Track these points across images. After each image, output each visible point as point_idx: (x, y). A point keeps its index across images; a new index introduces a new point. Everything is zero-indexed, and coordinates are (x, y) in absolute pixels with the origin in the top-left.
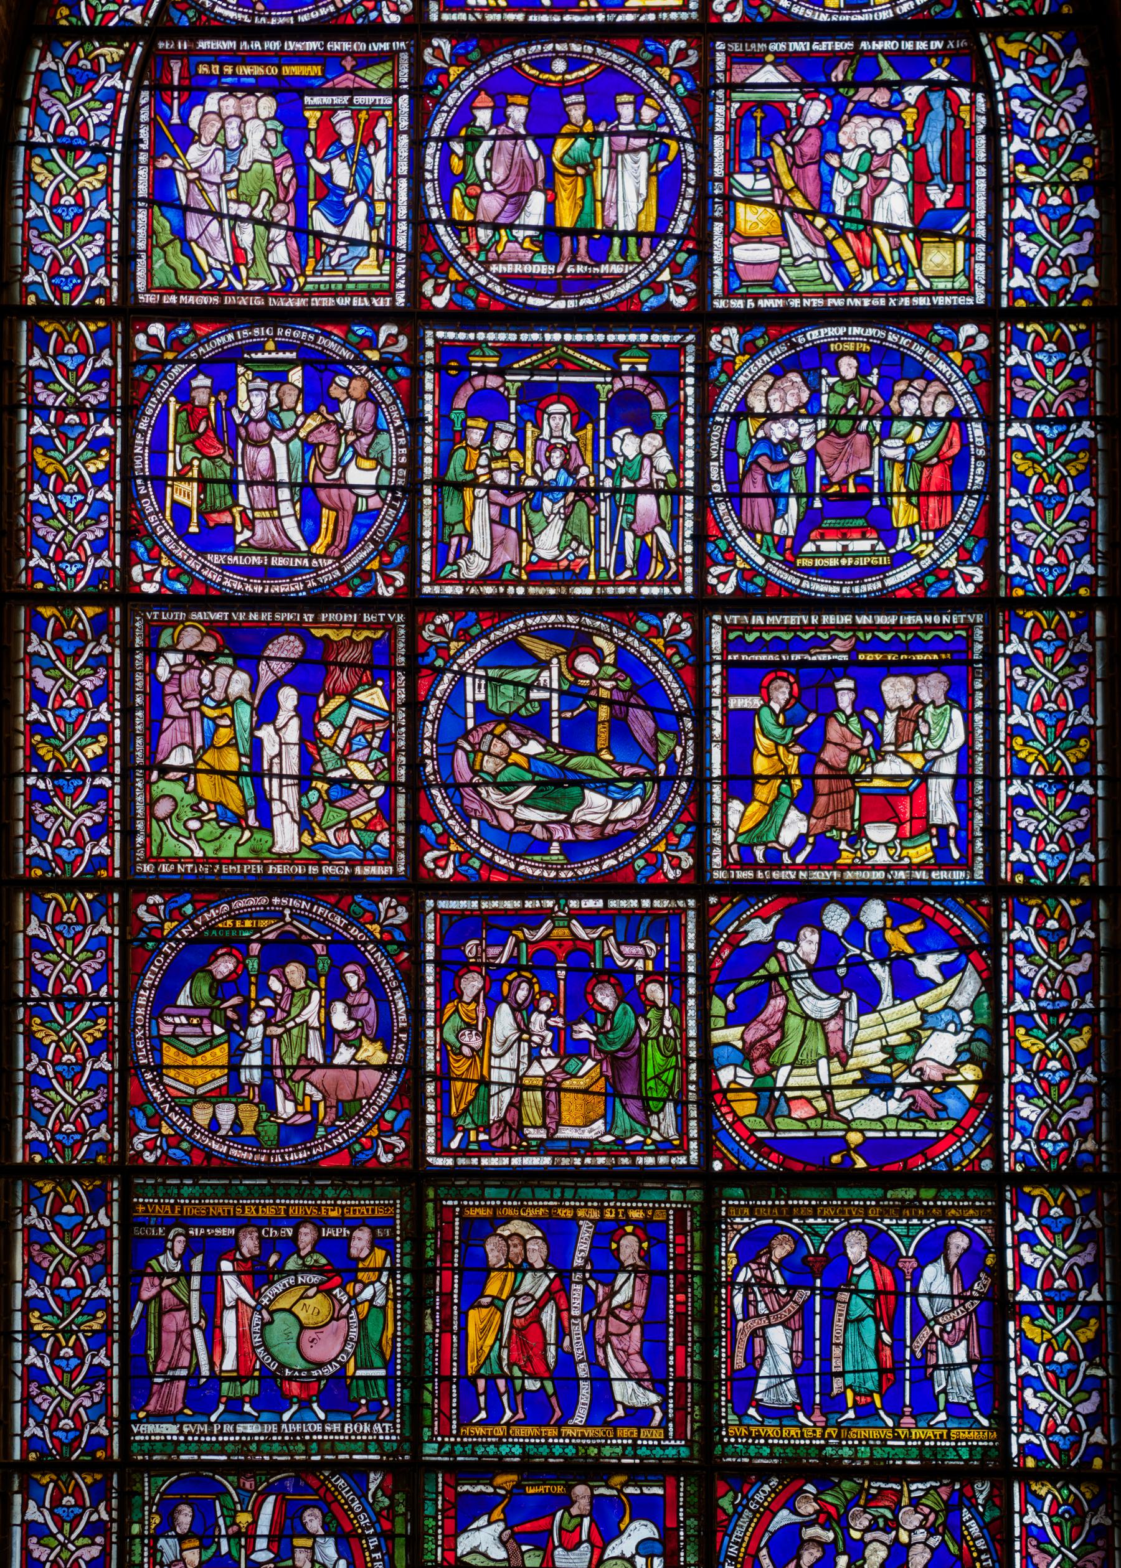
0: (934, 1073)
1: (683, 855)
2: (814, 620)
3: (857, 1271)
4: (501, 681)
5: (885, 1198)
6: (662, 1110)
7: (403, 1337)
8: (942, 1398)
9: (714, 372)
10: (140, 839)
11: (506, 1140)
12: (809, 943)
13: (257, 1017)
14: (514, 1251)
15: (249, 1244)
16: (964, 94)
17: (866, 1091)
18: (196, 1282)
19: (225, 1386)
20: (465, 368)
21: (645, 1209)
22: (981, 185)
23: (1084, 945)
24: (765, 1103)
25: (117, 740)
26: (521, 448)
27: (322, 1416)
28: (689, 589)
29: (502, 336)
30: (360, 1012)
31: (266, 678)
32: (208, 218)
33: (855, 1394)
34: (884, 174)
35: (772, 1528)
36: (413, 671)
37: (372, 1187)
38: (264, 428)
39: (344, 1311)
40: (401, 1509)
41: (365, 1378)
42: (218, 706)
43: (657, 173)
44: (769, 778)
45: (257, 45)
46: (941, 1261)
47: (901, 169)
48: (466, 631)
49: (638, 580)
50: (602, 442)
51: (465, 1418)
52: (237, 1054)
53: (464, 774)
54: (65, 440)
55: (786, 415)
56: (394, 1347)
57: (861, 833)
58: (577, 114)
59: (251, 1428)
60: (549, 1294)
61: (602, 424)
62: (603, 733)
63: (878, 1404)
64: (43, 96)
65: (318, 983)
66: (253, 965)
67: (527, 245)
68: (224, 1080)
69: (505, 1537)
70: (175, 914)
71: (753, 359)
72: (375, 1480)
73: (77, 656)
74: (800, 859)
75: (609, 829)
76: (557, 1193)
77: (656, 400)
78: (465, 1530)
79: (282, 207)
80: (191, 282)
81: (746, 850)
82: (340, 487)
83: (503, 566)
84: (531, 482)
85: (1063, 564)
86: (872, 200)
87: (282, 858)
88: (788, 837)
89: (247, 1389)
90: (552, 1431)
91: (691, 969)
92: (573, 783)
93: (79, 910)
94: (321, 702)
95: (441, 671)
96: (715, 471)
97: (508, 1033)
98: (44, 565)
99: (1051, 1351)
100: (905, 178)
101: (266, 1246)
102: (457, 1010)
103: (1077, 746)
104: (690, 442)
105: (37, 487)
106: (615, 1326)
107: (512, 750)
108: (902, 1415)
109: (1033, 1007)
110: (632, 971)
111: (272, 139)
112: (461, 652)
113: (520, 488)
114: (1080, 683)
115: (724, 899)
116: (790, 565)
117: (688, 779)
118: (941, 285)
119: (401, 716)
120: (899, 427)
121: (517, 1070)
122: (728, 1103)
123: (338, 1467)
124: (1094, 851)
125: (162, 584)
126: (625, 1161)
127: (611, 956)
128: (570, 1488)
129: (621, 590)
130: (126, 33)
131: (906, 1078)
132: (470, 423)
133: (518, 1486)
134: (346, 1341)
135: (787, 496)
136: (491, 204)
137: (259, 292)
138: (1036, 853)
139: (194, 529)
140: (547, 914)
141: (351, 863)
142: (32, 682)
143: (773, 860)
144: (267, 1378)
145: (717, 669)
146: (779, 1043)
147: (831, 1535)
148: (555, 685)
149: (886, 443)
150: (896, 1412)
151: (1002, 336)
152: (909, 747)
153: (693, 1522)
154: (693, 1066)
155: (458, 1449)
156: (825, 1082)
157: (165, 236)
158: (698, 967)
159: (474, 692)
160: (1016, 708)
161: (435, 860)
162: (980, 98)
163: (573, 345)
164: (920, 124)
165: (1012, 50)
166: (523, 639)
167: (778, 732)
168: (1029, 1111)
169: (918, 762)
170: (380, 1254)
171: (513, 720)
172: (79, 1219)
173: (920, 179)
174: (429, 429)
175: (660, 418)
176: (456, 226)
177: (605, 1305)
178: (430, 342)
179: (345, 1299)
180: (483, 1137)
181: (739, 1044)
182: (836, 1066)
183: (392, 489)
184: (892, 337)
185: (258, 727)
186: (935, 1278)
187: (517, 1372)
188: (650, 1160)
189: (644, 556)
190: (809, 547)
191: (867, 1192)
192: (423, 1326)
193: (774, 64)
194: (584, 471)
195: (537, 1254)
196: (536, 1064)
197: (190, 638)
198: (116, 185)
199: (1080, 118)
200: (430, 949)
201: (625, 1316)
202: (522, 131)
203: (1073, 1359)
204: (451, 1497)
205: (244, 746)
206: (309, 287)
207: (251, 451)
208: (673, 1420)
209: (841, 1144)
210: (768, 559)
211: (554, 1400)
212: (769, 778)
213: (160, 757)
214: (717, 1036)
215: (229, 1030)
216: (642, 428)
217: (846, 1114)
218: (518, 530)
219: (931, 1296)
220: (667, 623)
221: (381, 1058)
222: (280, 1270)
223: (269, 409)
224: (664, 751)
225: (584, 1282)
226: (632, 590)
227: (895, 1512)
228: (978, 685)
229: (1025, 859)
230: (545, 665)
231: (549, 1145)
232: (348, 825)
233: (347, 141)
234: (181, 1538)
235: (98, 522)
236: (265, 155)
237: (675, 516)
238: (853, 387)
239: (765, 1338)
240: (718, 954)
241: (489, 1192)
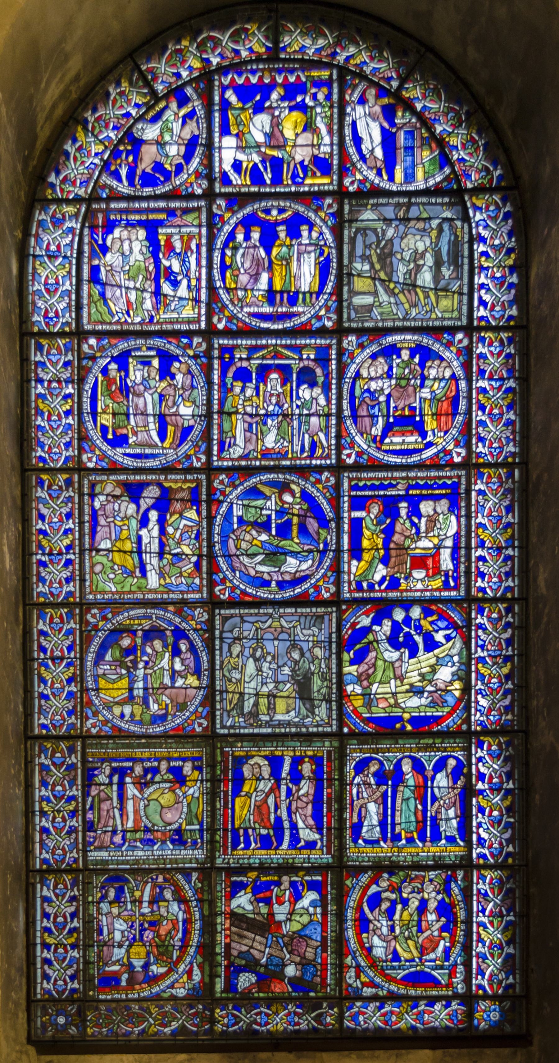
0: (442, 686)
1: (331, 586)
2: (390, 475)
3: (407, 777)
4: (248, 506)
7: (207, 811)
9: (345, 358)
10: (88, 583)
12: (387, 626)
13: (141, 665)
14: (256, 771)
15: (138, 770)
16: (459, 223)
17: (411, 694)
18: (115, 787)
20: (232, 358)
22: (466, 268)
23: (508, 625)
24: (367, 700)
25: (77, 536)
26: (258, 394)
27: (171, 847)
28: (334, 461)
29: (249, 342)
30: (187, 662)
31: (143, 507)
32: (115, 288)
33: (406, 832)
34: (421, 262)
36: (209, 502)
37: (192, 742)
38: (142, 388)
41: (190, 831)
42: (122, 520)
43: (320, 263)
44: (369, 550)
45: (137, 205)
47: (429, 260)
48: (233, 483)
49: (311, 457)
50: (294, 392)
51: (234, 847)
52: (132, 682)
53: (233, 550)
54: (51, 394)
55: (377, 378)
57: (410, 575)
58: (282, 235)
59: (140, 853)
60: (271, 790)
61: (294, 384)
62: (295, 529)
63: (416, 836)
64: (40, 231)
65: (167, 648)
66: (139, 641)
67: (260, 298)
68: (127, 695)
70: (104, 618)
71: (362, 352)
72: (195, 876)
73: (58, 498)
74: (383, 587)
75: (297, 575)
76: (275, 744)
77: (319, 371)
79: (149, 282)
80: (107, 318)
81: (359, 584)
82: (176, 415)
83: (250, 452)
84: (262, 412)
85: (501, 447)
86: (416, 275)
87: (151, 591)
88: (377, 577)
89: (138, 835)
90: (272, 852)
92: (282, 554)
93: (61, 617)
94: (168, 517)
95: (222, 502)
96: (345, 404)
98: (43, 455)
99: (491, 811)
100: (431, 265)
101: (146, 771)
103: (506, 532)
104: (334, 391)
105: (39, 418)
106: (300, 804)
107: (254, 538)
109: (486, 653)
111: (144, 250)
112: (231, 493)
113: (257, 415)
114: (508, 503)
116: (379, 449)
117: (333, 551)
118: (447, 315)
119: (205, 523)
120: (428, 383)
122: (350, 701)
123: (178, 870)
124: (513, 581)
125: (96, 463)
128: (280, 878)
129: (303, 462)
130: (78, 200)
131: (429, 688)
132: (235, 384)
133: (258, 877)
135: (377, 416)
136: (244, 279)
137: (139, 323)
138: (488, 582)
139: (110, 436)
140: (271, 616)
141: (182, 592)
142: (38, 510)
143: (371, 587)
145: (346, 499)
146: (373, 673)
148: (273, 508)
149: (423, 390)
151: (475, 339)
152: (432, 534)
154: (334, 686)
155: (231, 861)
156: (394, 691)
157: (96, 296)
159: (237, 511)
160: (479, 515)
161: (220, 591)
162: (466, 226)
163: (282, 346)
164: (439, 237)
165: (479, 203)
166: (259, 486)
167: (373, 528)
168: (483, 702)
169: (436, 541)
170: (196, 773)
171: (255, 524)
172: (63, 759)
173: (438, 264)
174: (216, 387)
175: (321, 380)
176: (228, 290)
178: (216, 346)
180: (241, 720)
181: (356, 674)
182: (398, 683)
183: (200, 416)
184: (425, 341)
185: (140, 528)
186: (442, 780)
187: (257, 826)
189: (313, 446)
190: (387, 440)
191: (412, 741)
193: (371, 209)
194: (286, 406)
196: (264, 686)
197: (109, 489)
198: (74, 273)
199: (510, 235)
201: (305, 799)
202: (258, 244)
203: (501, 815)
205: (134, 539)
206: (161, 320)
207: (136, 399)
209: (400, 719)
210: (369, 446)
211: (273, 839)
212: (369, 550)
213: (96, 545)
214: (346, 670)
215: (129, 672)
216: (312, 384)
217: (402, 705)
218: (257, 435)
219: (439, 788)
220: (324, 478)
221: (196, 683)
222: (152, 782)
223: (144, 379)
224: (322, 538)
225: (287, 784)
226: (308, 462)
227: (422, 885)
228: (463, 504)
229: (483, 586)
230: (269, 498)
232: (181, 575)
233: (178, 251)
235: (67, 434)
236: (141, 258)
237: (327, 427)
238: (408, 364)
239: (366, 808)
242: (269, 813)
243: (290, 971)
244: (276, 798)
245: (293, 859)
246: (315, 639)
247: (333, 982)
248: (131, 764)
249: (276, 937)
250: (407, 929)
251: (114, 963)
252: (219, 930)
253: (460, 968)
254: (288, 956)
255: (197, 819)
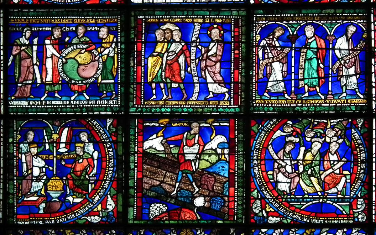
3: (310, 41)
5: (321, 13)
7: (121, 68)
8: (344, 88)
15: (57, 33)
18: (35, 48)
19: (47, 87)
21: (222, 19)
27: (87, 98)
35: (273, 137)
37: (108, 11)
39: (97, 58)
40: (120, 132)
46: (345, 36)
56: (117, 72)
59: (58, 103)
60: (182, 51)
69: (163, 142)
72: (109, 122)
78: (147, 140)
89: (56, 88)
90: (183, 103)
101: (64, 34)
108: (328, 94)
128: (190, 124)
133: (169, 123)
134: (97, 70)
144: (64, 83)
147: (298, 140)
150: (326, 94)
153: (241, 136)
155: (144, 110)
170: (111, 37)
177: (205, 55)
179: (97, 54)
187: (168, 81)
191: (314, 11)
192: (130, 64)
195: (177, 36)
201: (213, 59)
204: (141, 127)
208: (233, 98)
222: (70, 43)
225: (196, 46)
234: (30, 144)
241: (157, 13)
242: (180, 70)
243: (199, 202)
244: (186, 58)
245: (202, 108)
247: (240, 212)
248: (50, 29)
249: (186, 174)
250: (310, 168)
251: (33, 195)
252: (132, 167)
253: (360, 201)
254: (197, 190)
255: (112, 75)
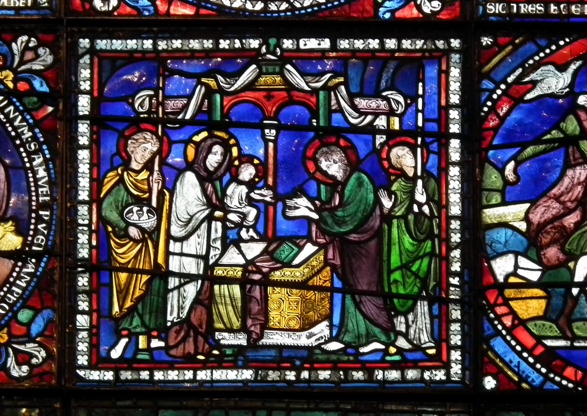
6: (412, 309)
11: (190, 347)
24: (557, 301)
91: (455, 128)
97: (193, 210)
102: (121, 181)
110: (371, 130)
115: (502, 40)
121: (205, 258)
122: (506, 302)
126: (358, 375)
127: (340, 110)
140: (253, 57)
154: (456, 253)
158: (464, 121)
180: (156, 343)
181: (523, 226)
188: (394, 375)
196: (232, 251)
200: (84, 104)
214: (491, 214)
231: (250, 354)
240: (493, 110)
246: (396, 124)
